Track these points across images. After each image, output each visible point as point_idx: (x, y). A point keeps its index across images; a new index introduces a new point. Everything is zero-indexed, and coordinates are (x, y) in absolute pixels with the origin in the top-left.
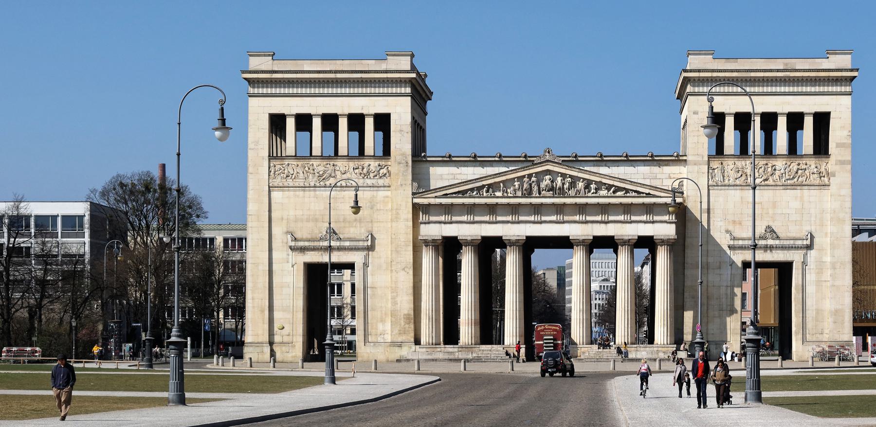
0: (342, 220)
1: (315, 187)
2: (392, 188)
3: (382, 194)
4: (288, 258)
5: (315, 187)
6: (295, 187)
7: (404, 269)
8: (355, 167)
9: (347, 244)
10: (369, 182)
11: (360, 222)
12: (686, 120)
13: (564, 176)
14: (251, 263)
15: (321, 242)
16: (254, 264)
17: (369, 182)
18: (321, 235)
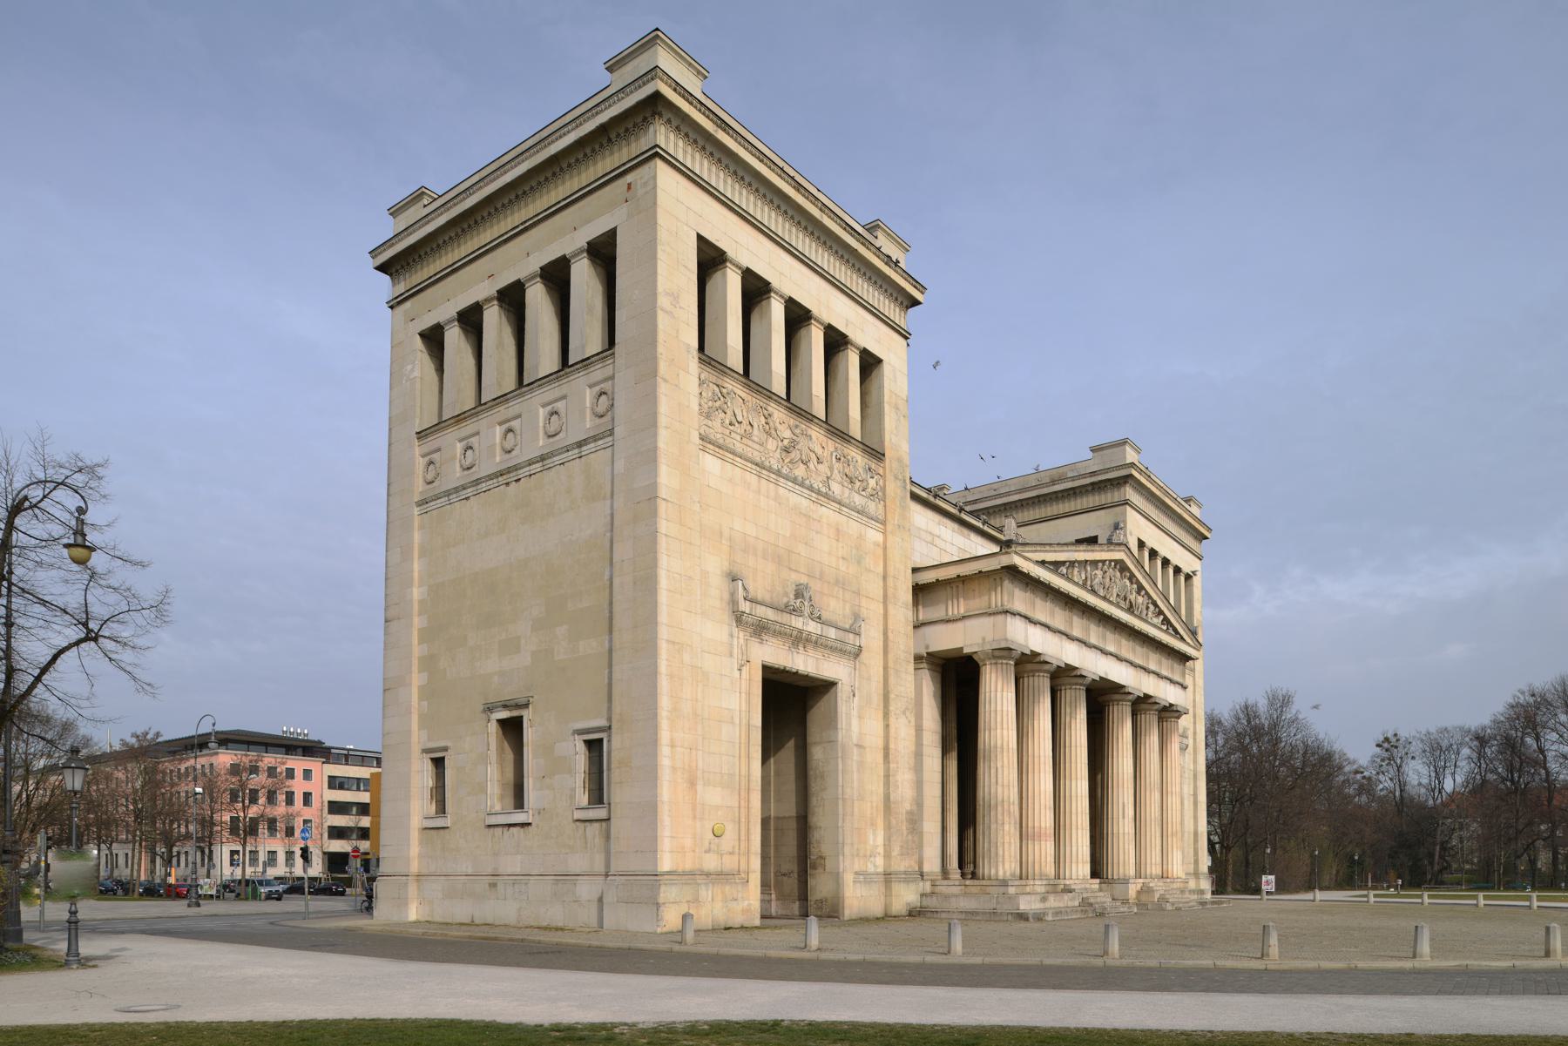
0: (818, 576)
1: (778, 473)
2: (889, 528)
3: (873, 535)
4: (731, 645)
5: (778, 473)
6: (746, 460)
7: (904, 713)
8: (838, 456)
9: (832, 633)
10: (858, 500)
11: (843, 588)
12: (1079, 542)
13: (1132, 578)
14: (668, 641)
15: (793, 617)
16: (674, 643)
17: (858, 500)
18: (785, 600)
